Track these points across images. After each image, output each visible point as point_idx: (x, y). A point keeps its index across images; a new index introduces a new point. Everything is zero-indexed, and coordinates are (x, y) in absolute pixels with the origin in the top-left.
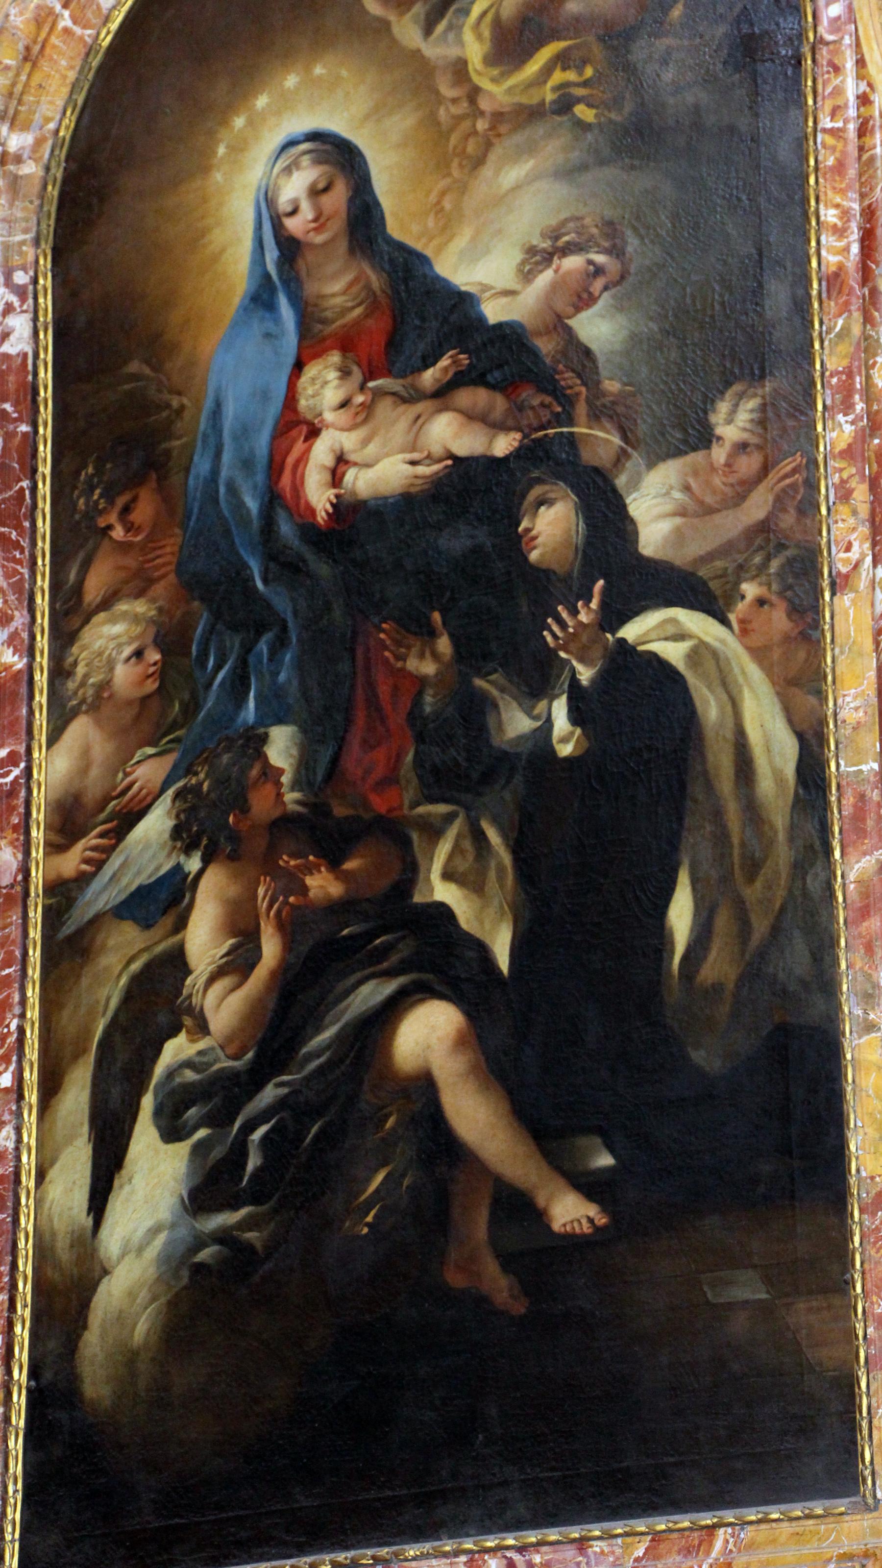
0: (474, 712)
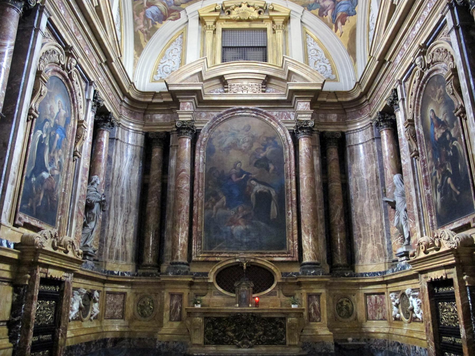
0: (447, 153)
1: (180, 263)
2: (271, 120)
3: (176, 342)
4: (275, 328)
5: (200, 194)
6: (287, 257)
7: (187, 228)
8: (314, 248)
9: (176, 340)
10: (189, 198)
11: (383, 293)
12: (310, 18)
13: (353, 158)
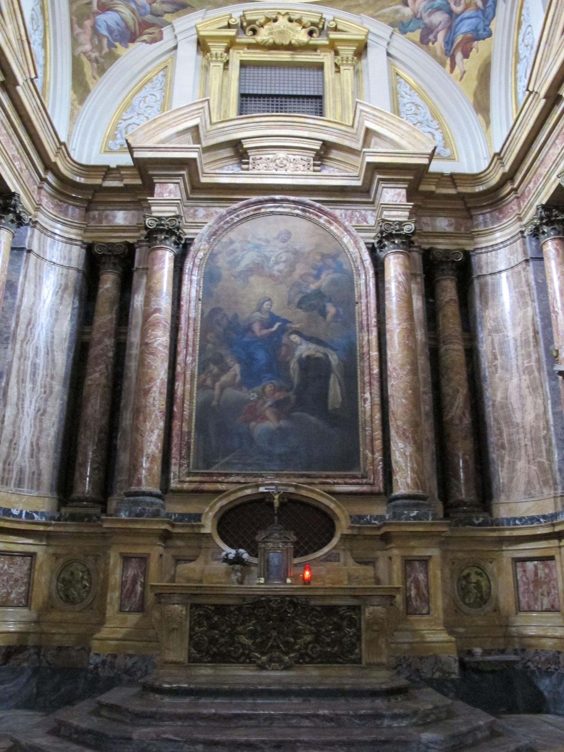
1: (144, 494)
2: (330, 223)
3: (131, 656)
4: (338, 628)
5: (189, 359)
6: (362, 484)
7: (162, 424)
8: (415, 466)
9: (131, 652)
10: (166, 365)
11: (552, 558)
12: (405, 46)
13: (486, 297)
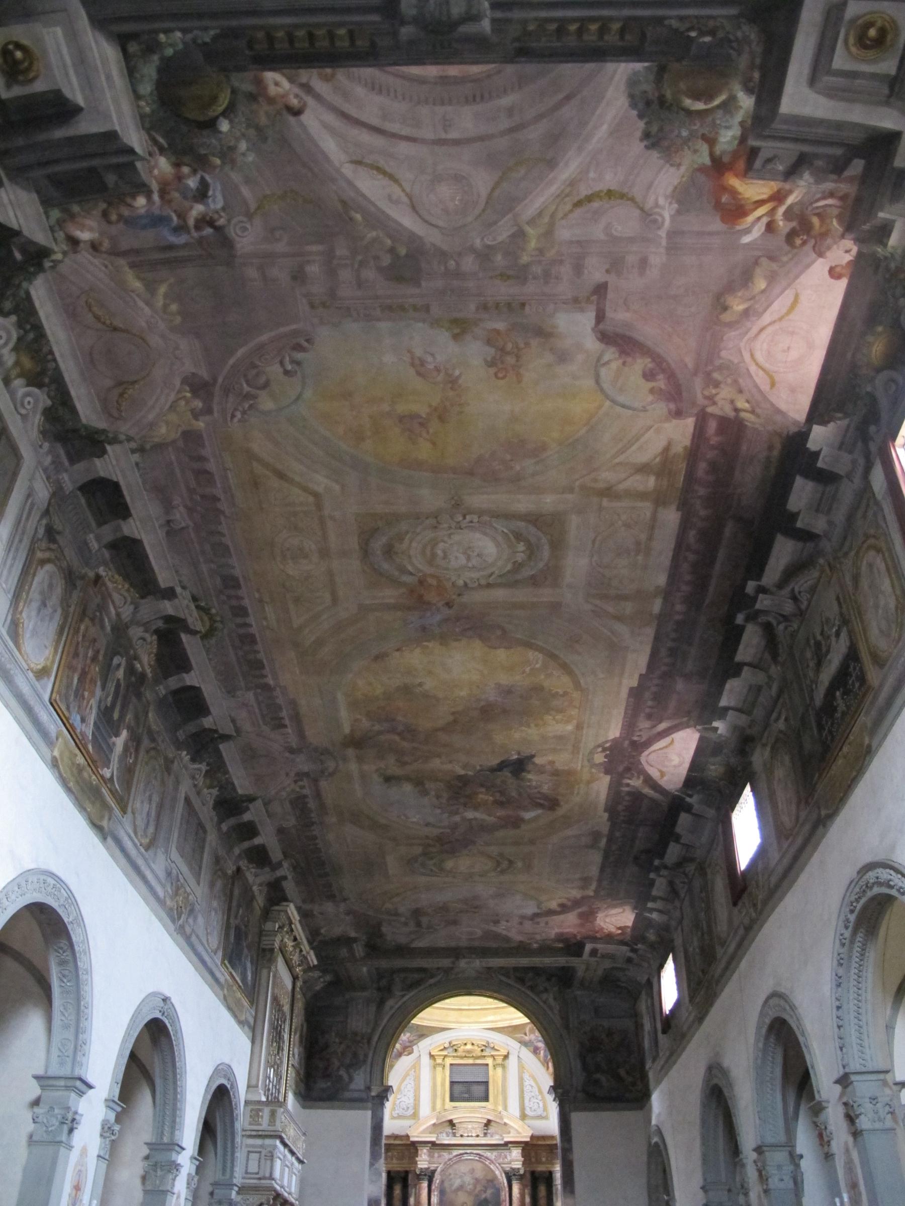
12: (526, 1054)
